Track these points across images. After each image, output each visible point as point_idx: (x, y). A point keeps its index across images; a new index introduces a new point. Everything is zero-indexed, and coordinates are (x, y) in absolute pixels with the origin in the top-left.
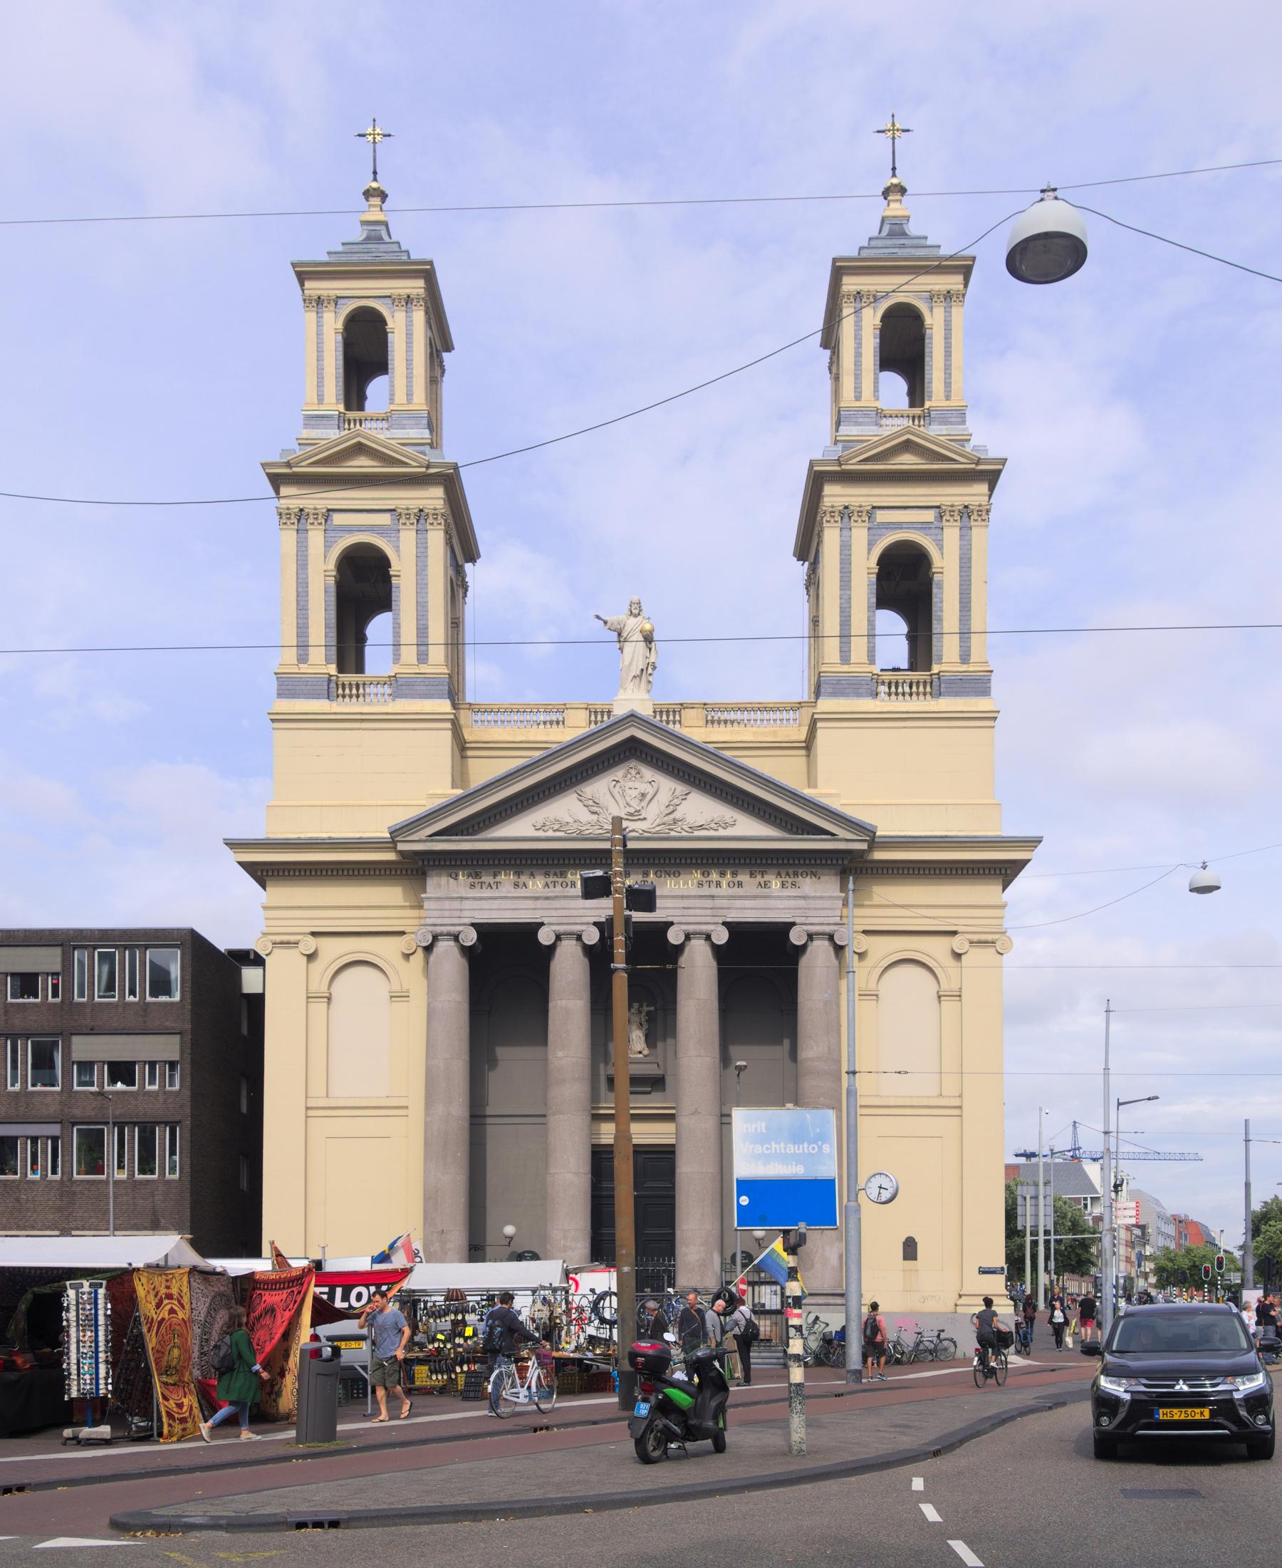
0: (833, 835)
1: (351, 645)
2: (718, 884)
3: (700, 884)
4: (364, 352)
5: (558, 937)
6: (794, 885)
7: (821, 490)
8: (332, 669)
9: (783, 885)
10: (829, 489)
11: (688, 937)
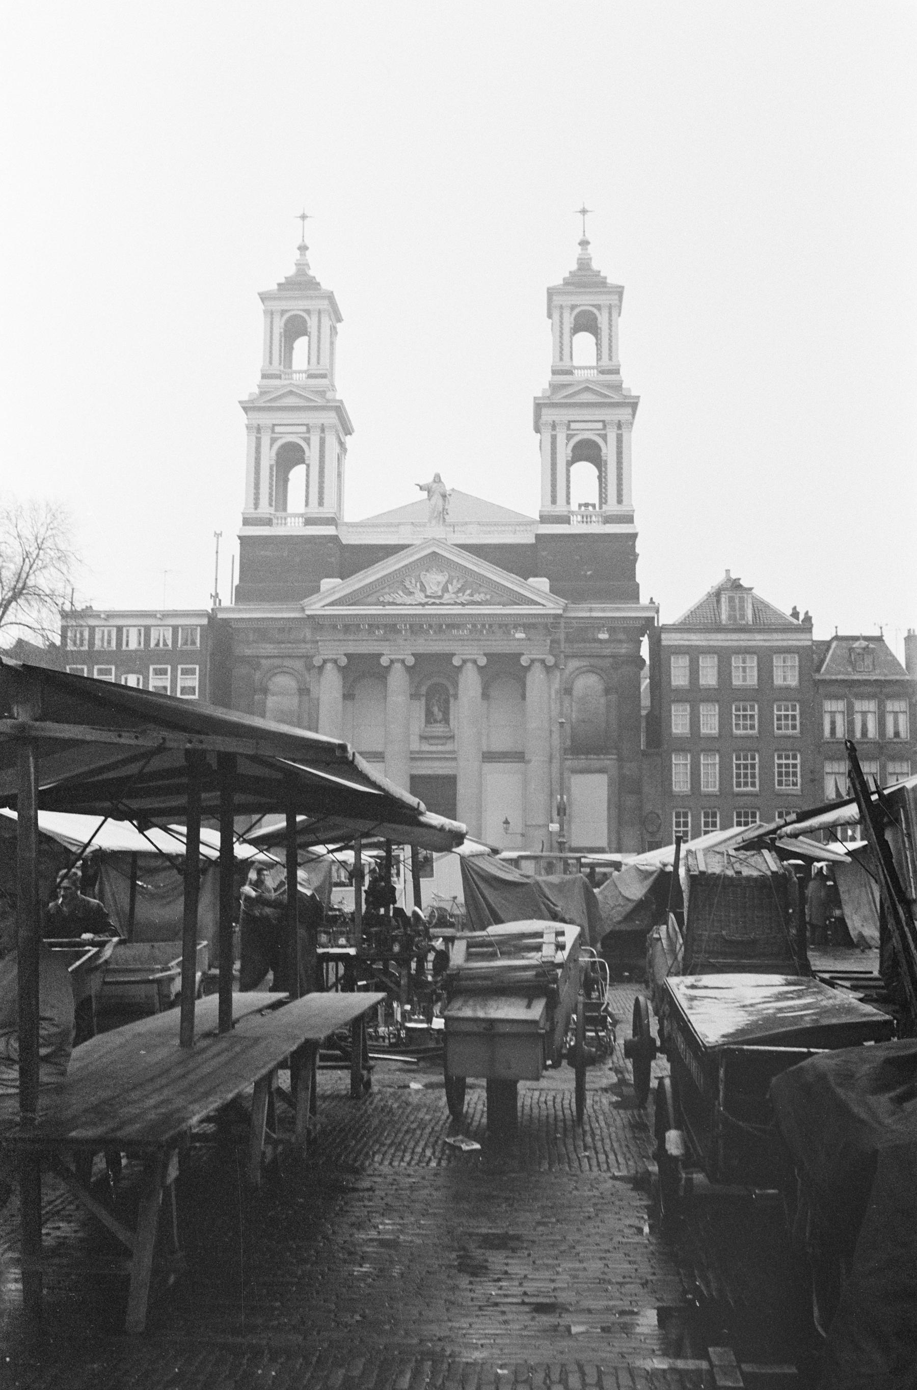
2: (482, 632)
5: (392, 661)
10: (544, 411)
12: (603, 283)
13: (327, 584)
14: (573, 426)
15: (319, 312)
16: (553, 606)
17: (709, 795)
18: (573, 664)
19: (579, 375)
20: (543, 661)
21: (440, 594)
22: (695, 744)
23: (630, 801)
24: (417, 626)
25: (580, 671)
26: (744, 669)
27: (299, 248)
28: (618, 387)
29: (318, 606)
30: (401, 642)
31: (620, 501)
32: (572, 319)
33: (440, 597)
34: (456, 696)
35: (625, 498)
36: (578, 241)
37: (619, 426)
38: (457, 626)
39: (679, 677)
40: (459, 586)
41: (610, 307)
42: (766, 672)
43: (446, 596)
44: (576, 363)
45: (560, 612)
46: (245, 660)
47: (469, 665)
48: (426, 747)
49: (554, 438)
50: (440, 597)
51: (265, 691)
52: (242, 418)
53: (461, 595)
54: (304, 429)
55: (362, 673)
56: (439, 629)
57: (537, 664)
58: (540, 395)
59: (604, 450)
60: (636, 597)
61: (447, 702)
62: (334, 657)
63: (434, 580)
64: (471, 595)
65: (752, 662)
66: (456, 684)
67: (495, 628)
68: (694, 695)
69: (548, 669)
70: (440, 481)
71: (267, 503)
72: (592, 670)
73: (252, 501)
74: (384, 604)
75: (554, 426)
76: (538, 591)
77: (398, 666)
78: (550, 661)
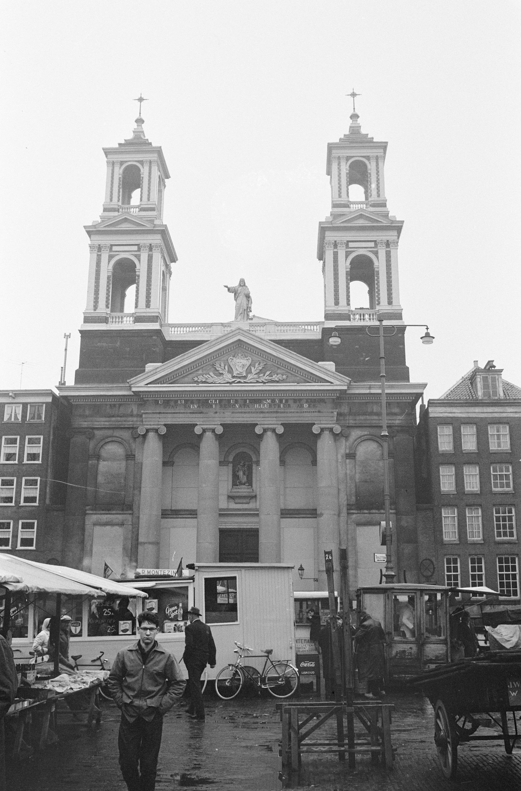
0: (332, 383)
1: (118, 300)
2: (279, 406)
3: (270, 406)
4: (130, 180)
5: (204, 431)
6: (314, 406)
7: (324, 234)
8: (108, 311)
9: (309, 406)
10: (327, 233)
11: (265, 431)
12: (371, 141)
13: (150, 367)
14: (351, 245)
15: (150, 162)
16: (339, 383)
17: (474, 544)
18: (355, 434)
19: (353, 207)
20: (331, 430)
21: (244, 374)
22: (461, 500)
23: (408, 549)
24: (226, 400)
25: (362, 440)
26: (498, 436)
27: (136, 121)
28: (386, 215)
29: (143, 384)
30: (212, 414)
31: (390, 303)
32: (348, 167)
33: (245, 377)
34: (258, 463)
35: (394, 301)
36: (350, 115)
37: (388, 244)
38: (259, 401)
39: (444, 443)
40: (260, 368)
41: (377, 158)
43: (250, 376)
44: (351, 199)
45: (345, 388)
46: (81, 431)
47: (269, 433)
48: (232, 505)
50: (245, 377)
51: (98, 457)
52: (87, 240)
53: (262, 375)
54: (135, 248)
55: (179, 442)
56: (244, 404)
57: (326, 433)
58: (324, 220)
59: (376, 263)
60: (406, 378)
61: (250, 468)
62: (155, 427)
63: (240, 364)
64: (270, 375)
66: (257, 452)
67: (290, 402)
68: (458, 459)
69: (336, 436)
70: (244, 285)
71: (105, 306)
72: (372, 438)
73: (92, 303)
74: (197, 382)
75: (335, 245)
76: (326, 371)
77: (209, 434)
78: (337, 429)
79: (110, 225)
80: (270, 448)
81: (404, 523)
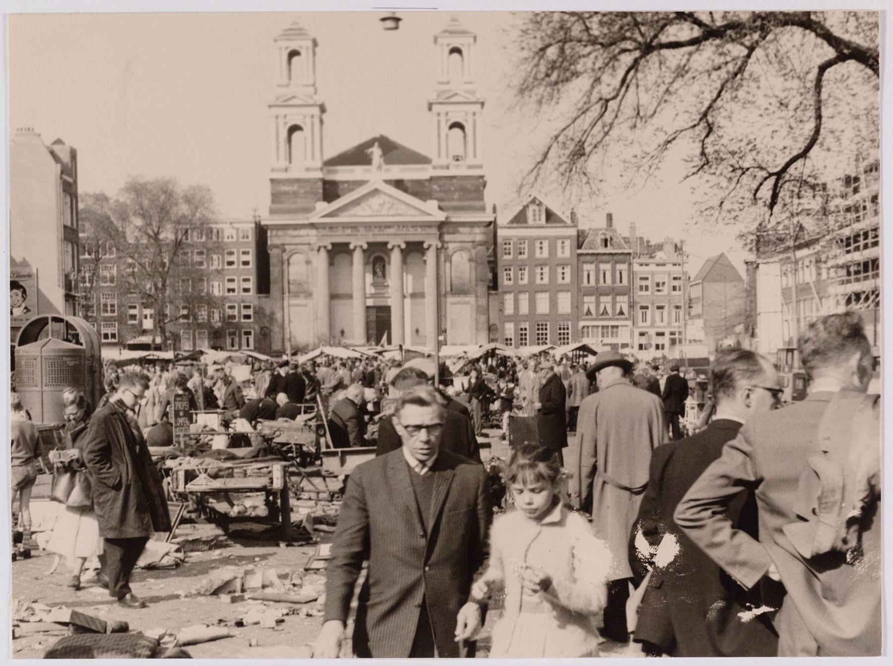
16: (441, 216)
31: (475, 156)
34: (389, 263)
42: (553, 250)
49: (439, 122)
61: (384, 266)
65: (546, 244)
66: (389, 257)
79: (286, 101)
80: (395, 257)
81: (480, 303)
